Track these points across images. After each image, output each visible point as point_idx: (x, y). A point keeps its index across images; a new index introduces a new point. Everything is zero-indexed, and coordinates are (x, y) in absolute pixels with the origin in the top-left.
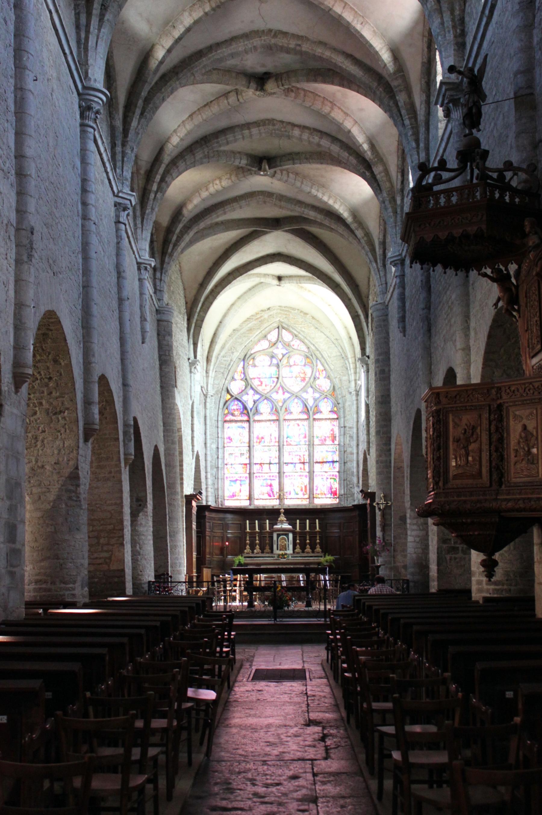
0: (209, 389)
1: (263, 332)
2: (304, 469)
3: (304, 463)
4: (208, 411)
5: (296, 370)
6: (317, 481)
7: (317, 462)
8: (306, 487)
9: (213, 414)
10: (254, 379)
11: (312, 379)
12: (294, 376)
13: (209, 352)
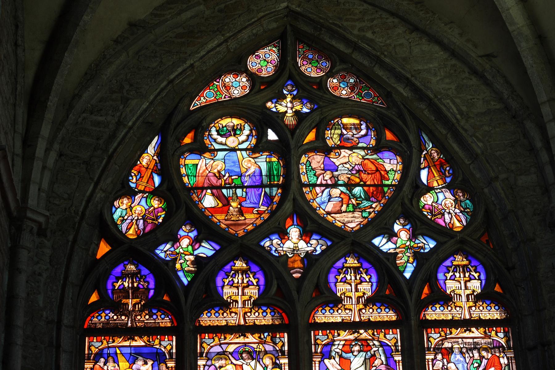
0: (32, 202)
1: (232, 45)
4: (22, 279)
5: (347, 160)
9: (41, 299)
10: (203, 188)
11: (406, 189)
12: (343, 179)
13: (37, 79)
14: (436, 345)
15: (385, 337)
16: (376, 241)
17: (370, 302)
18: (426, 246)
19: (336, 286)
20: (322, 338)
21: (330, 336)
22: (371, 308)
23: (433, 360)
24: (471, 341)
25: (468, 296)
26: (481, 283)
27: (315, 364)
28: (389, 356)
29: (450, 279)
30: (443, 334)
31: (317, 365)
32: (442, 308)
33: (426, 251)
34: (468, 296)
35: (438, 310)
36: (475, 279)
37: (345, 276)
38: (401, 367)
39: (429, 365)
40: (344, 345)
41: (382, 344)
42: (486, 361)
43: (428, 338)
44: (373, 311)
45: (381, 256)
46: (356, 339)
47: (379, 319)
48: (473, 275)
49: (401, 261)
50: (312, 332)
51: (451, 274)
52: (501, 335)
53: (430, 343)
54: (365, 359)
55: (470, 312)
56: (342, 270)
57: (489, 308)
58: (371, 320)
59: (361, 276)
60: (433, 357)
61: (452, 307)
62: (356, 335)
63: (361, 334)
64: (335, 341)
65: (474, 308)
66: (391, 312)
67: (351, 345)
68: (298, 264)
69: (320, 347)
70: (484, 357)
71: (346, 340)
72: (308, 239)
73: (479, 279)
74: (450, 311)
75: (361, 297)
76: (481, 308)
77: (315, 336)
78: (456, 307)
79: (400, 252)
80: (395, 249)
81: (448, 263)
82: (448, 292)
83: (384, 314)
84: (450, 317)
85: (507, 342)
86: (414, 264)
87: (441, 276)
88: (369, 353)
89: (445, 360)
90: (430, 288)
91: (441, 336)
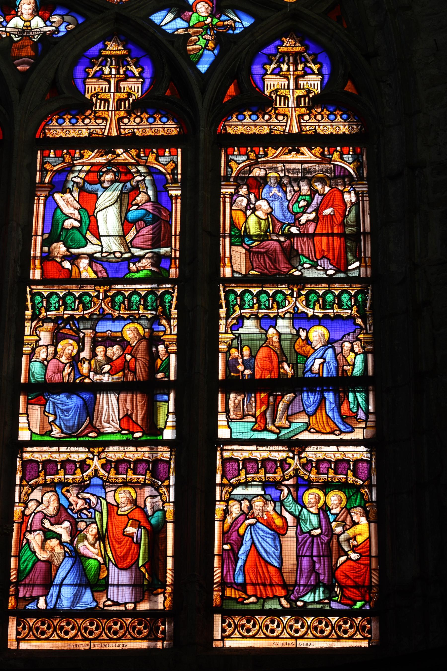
2: (152, 427)
3: (149, 389)
6: (237, 504)
7: (234, 384)
8: (156, 535)
14: (239, 172)
15: (157, 160)
16: (157, 18)
17: (137, 107)
18: (238, 25)
19: (84, 83)
20: (54, 161)
21: (68, 159)
22: (138, 116)
23: (232, 195)
24: (298, 166)
25: (298, 99)
26: (322, 81)
27: (39, 199)
28: (160, 188)
29: (272, 74)
30: (252, 155)
31: (42, 202)
32: (254, 117)
33: (236, 32)
34: (298, 99)
35: (248, 119)
36: (313, 73)
37: (101, 69)
38: (179, 206)
39: (224, 202)
40: (88, 172)
41: (151, 171)
42: (320, 198)
43: (228, 161)
44: (142, 121)
45: (160, 37)
46: (109, 163)
47: (149, 133)
48: (310, 68)
49: (194, 47)
50: (39, 152)
51: (273, 66)
52: (349, 158)
53: (229, 170)
54: (122, 192)
55: (300, 123)
56: (97, 59)
57: (332, 117)
58: (137, 134)
59: (127, 69)
60: (233, 191)
61: (270, 116)
62: (110, 156)
63: (118, 155)
64: (74, 165)
65: (306, 118)
66: (170, 122)
67: (100, 171)
68: (29, 51)
69: (49, 174)
70: (317, 191)
71: (92, 165)
72: (47, 15)
73: (320, 72)
74: (267, 121)
75: (124, 100)
76: (319, 117)
77: (42, 157)
78: (277, 115)
79: (194, 33)
80: (186, 29)
81: (270, 49)
82: (267, 92)
83: (158, 124)
84: (266, 130)
85: (358, 169)
86: (216, 52)
87: (257, 69)
88: (128, 184)
89: (252, 196)
90: (239, 88)
91: (248, 159)
